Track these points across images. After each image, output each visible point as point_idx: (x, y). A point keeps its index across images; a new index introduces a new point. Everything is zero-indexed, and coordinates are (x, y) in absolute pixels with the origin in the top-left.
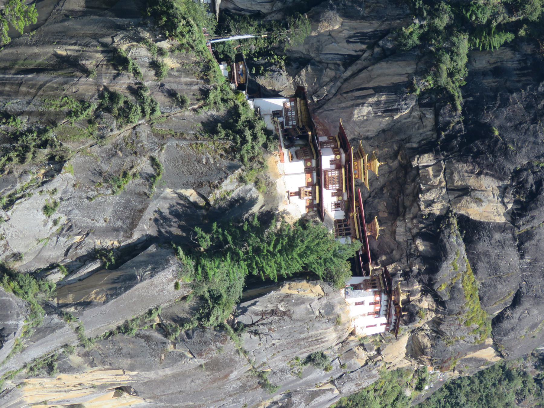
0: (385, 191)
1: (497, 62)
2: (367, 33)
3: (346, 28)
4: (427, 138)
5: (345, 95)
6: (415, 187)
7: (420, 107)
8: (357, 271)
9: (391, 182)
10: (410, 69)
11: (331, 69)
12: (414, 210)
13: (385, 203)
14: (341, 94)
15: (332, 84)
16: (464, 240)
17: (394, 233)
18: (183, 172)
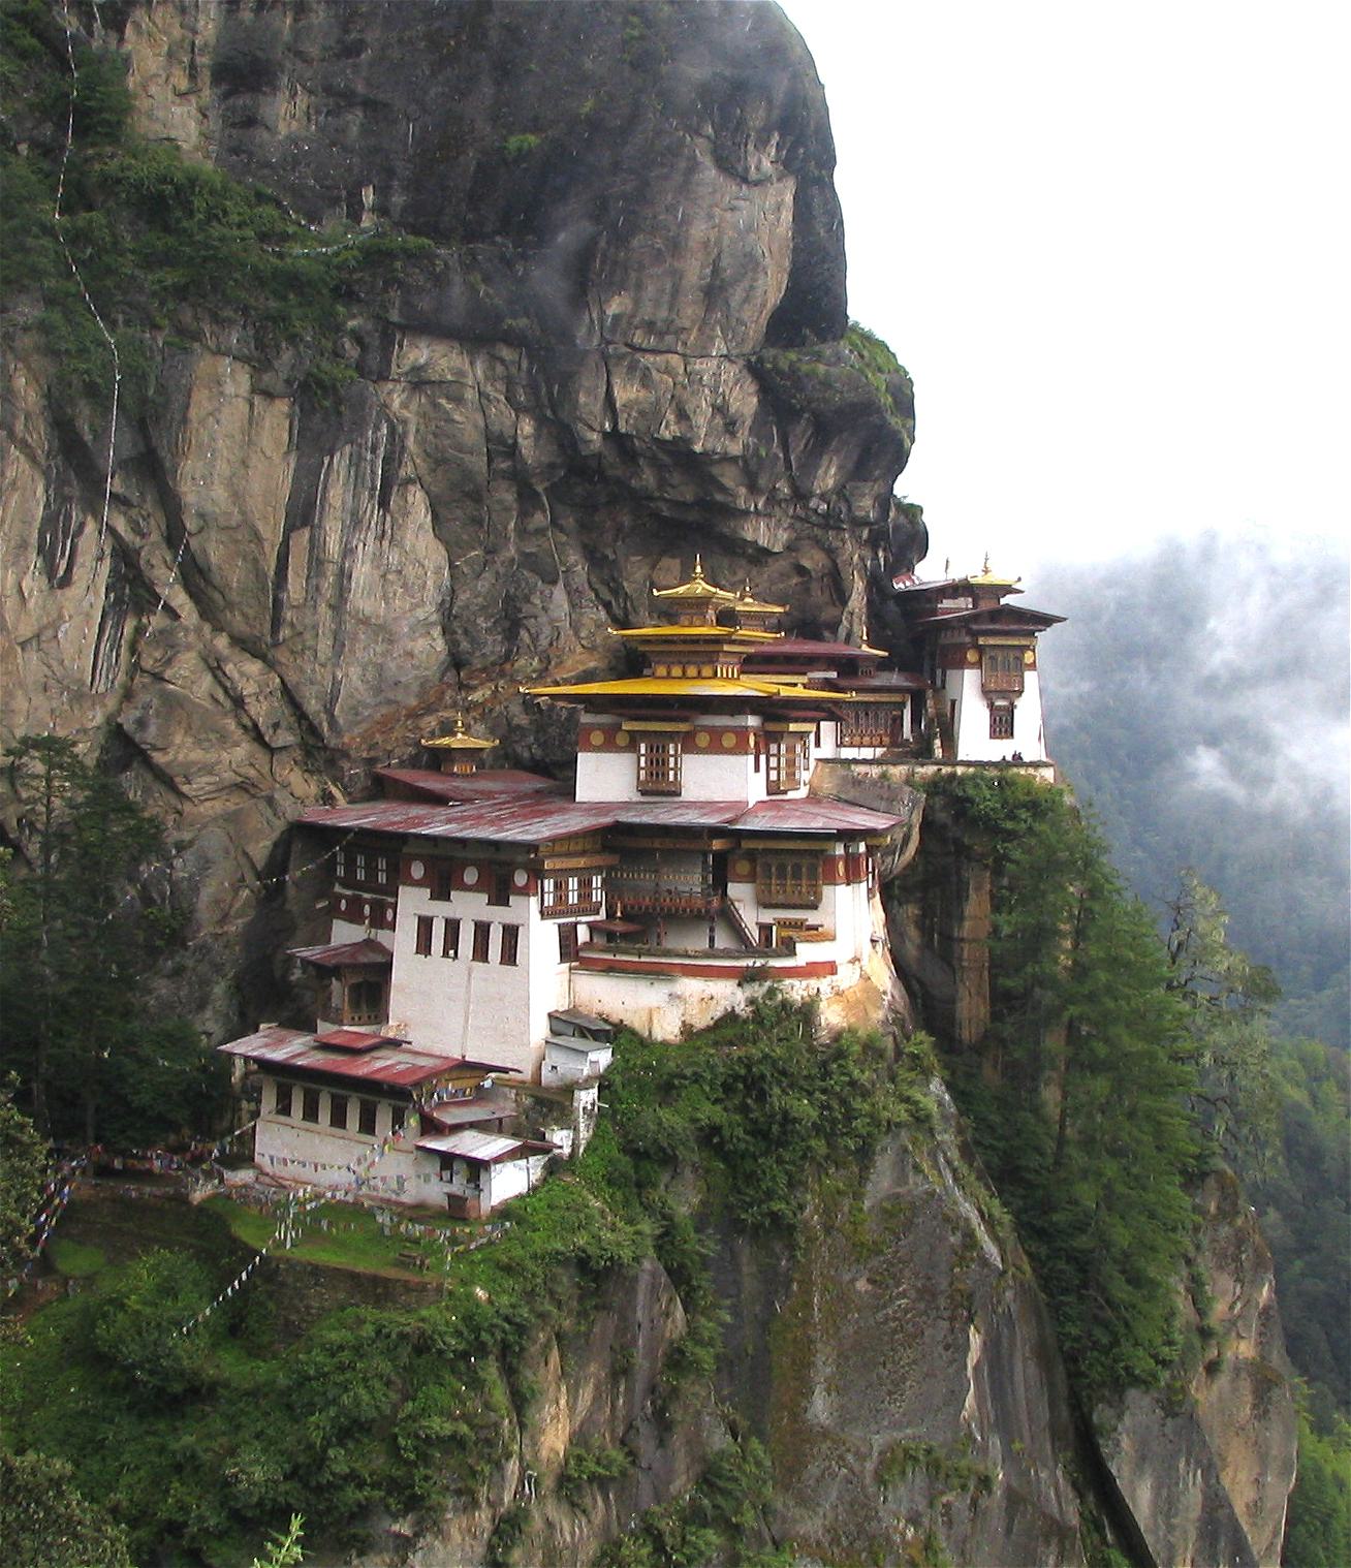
0: (609, 552)
1: (193, 66)
2: (47, 506)
3: (11, 578)
4: (510, 382)
5: (285, 632)
6: (654, 461)
7: (386, 379)
8: (896, 698)
9: (584, 527)
10: (237, 381)
11: (169, 662)
12: (729, 477)
13: (633, 559)
14: (276, 645)
15: (229, 668)
16: (824, 340)
17: (761, 555)
18: (915, 1362)
